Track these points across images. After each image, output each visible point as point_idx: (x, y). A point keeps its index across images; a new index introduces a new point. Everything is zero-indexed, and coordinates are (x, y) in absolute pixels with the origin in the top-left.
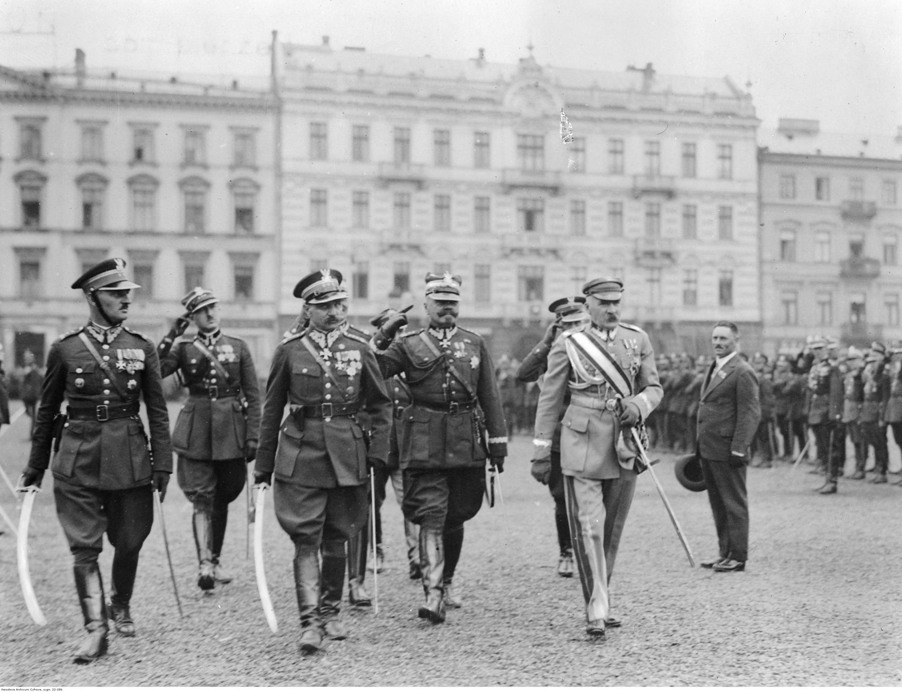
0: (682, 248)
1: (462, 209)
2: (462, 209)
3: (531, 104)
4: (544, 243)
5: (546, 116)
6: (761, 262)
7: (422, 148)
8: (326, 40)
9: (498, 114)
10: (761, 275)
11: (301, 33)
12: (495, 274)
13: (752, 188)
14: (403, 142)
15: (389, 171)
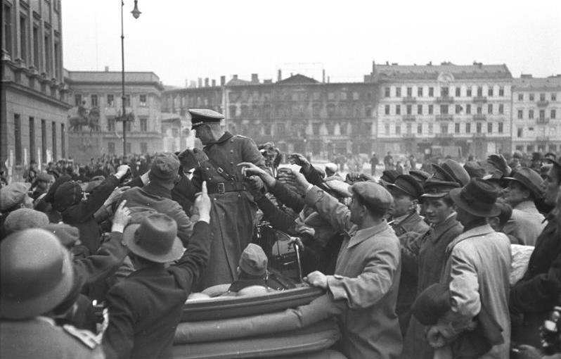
0: (489, 117)
1: (425, 109)
2: (425, 109)
3: (445, 79)
4: (448, 117)
5: (449, 82)
6: (512, 120)
7: (415, 93)
8: (387, 63)
9: (436, 82)
10: (511, 124)
11: (381, 61)
12: (434, 126)
13: (510, 99)
14: (409, 91)
15: (406, 100)
